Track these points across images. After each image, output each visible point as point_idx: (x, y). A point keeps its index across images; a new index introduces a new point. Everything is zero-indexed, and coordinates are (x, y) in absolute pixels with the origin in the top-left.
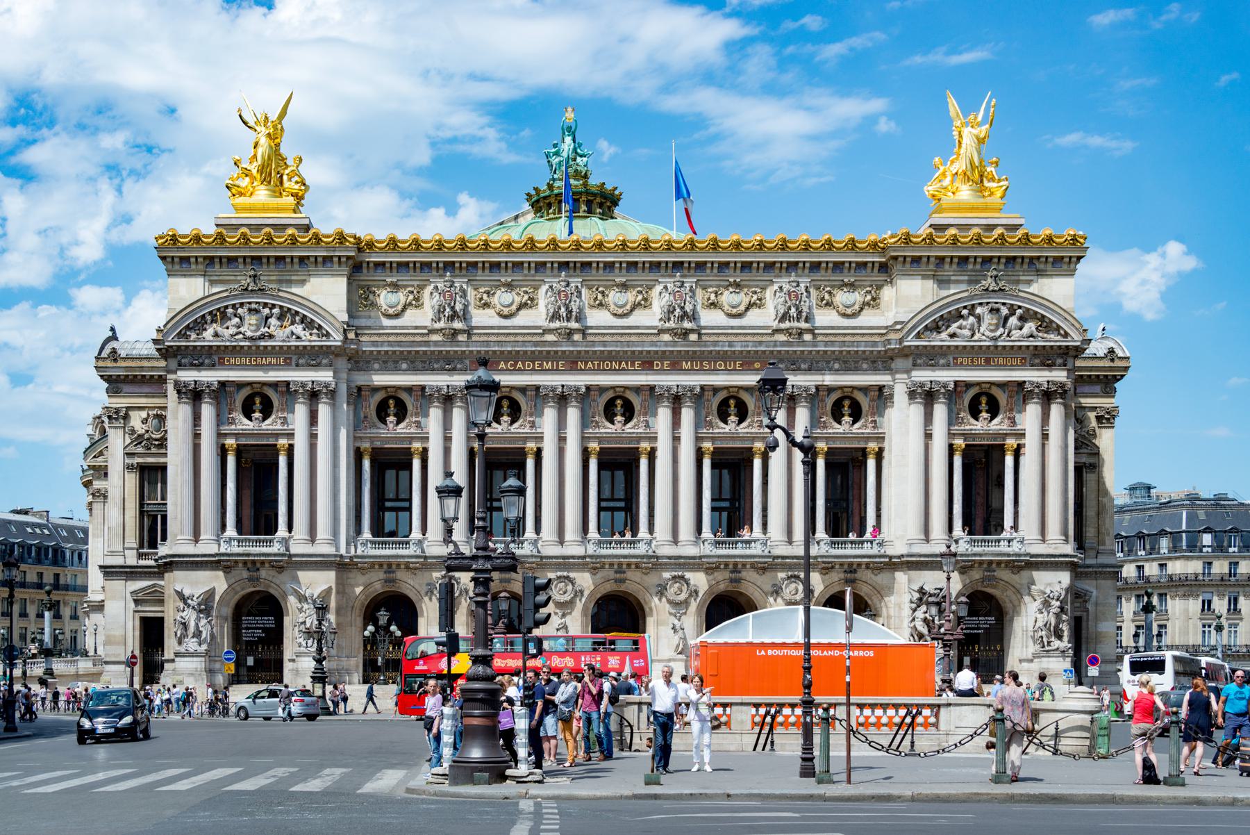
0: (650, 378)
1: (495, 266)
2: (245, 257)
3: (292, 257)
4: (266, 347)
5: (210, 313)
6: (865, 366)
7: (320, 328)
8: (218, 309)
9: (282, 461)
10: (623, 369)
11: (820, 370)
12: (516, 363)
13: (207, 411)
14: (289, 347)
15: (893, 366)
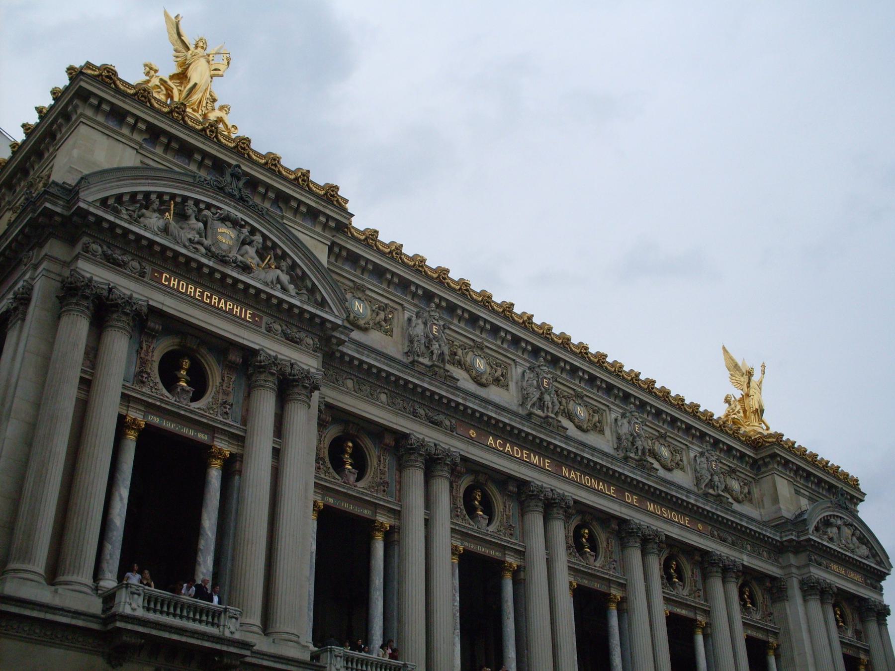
0: (624, 510)
1: (474, 320)
2: (205, 154)
3: (268, 187)
4: (236, 281)
5: (160, 195)
6: (765, 553)
7: (313, 290)
8: (173, 196)
9: (215, 475)
10: (601, 491)
11: (742, 549)
12: (504, 446)
13: (119, 346)
14: (270, 296)
15: (780, 560)
